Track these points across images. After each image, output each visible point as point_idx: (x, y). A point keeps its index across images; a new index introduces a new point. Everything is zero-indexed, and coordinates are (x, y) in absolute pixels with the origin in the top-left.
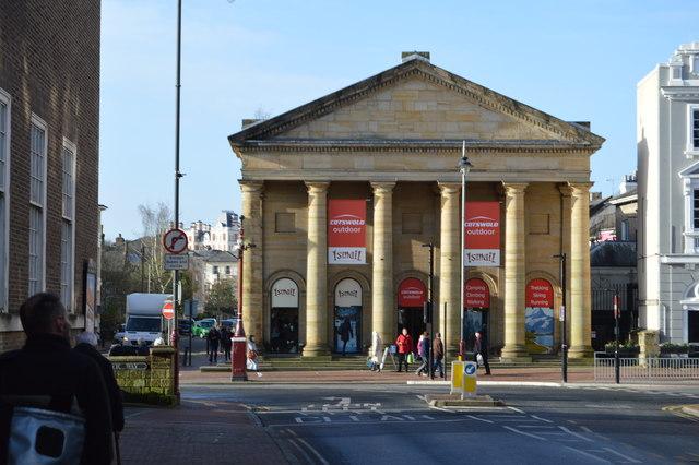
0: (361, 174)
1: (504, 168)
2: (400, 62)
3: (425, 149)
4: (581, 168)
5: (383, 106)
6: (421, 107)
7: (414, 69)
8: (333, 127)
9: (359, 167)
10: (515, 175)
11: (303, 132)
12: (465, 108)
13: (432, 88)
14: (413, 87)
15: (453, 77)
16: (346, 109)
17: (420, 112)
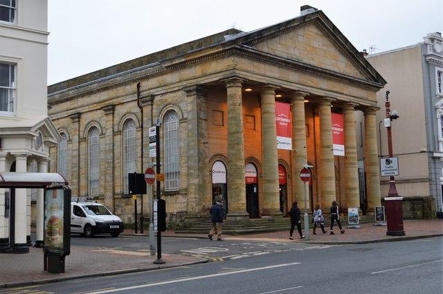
0: (293, 85)
1: (348, 93)
2: (297, 13)
3: (322, 72)
4: (374, 100)
5: (301, 39)
6: (316, 44)
7: (316, 20)
8: (278, 48)
9: (293, 80)
10: (352, 98)
11: (265, 48)
12: (332, 51)
13: (320, 33)
14: (312, 31)
15: (334, 28)
16: (285, 36)
17: (316, 48)
